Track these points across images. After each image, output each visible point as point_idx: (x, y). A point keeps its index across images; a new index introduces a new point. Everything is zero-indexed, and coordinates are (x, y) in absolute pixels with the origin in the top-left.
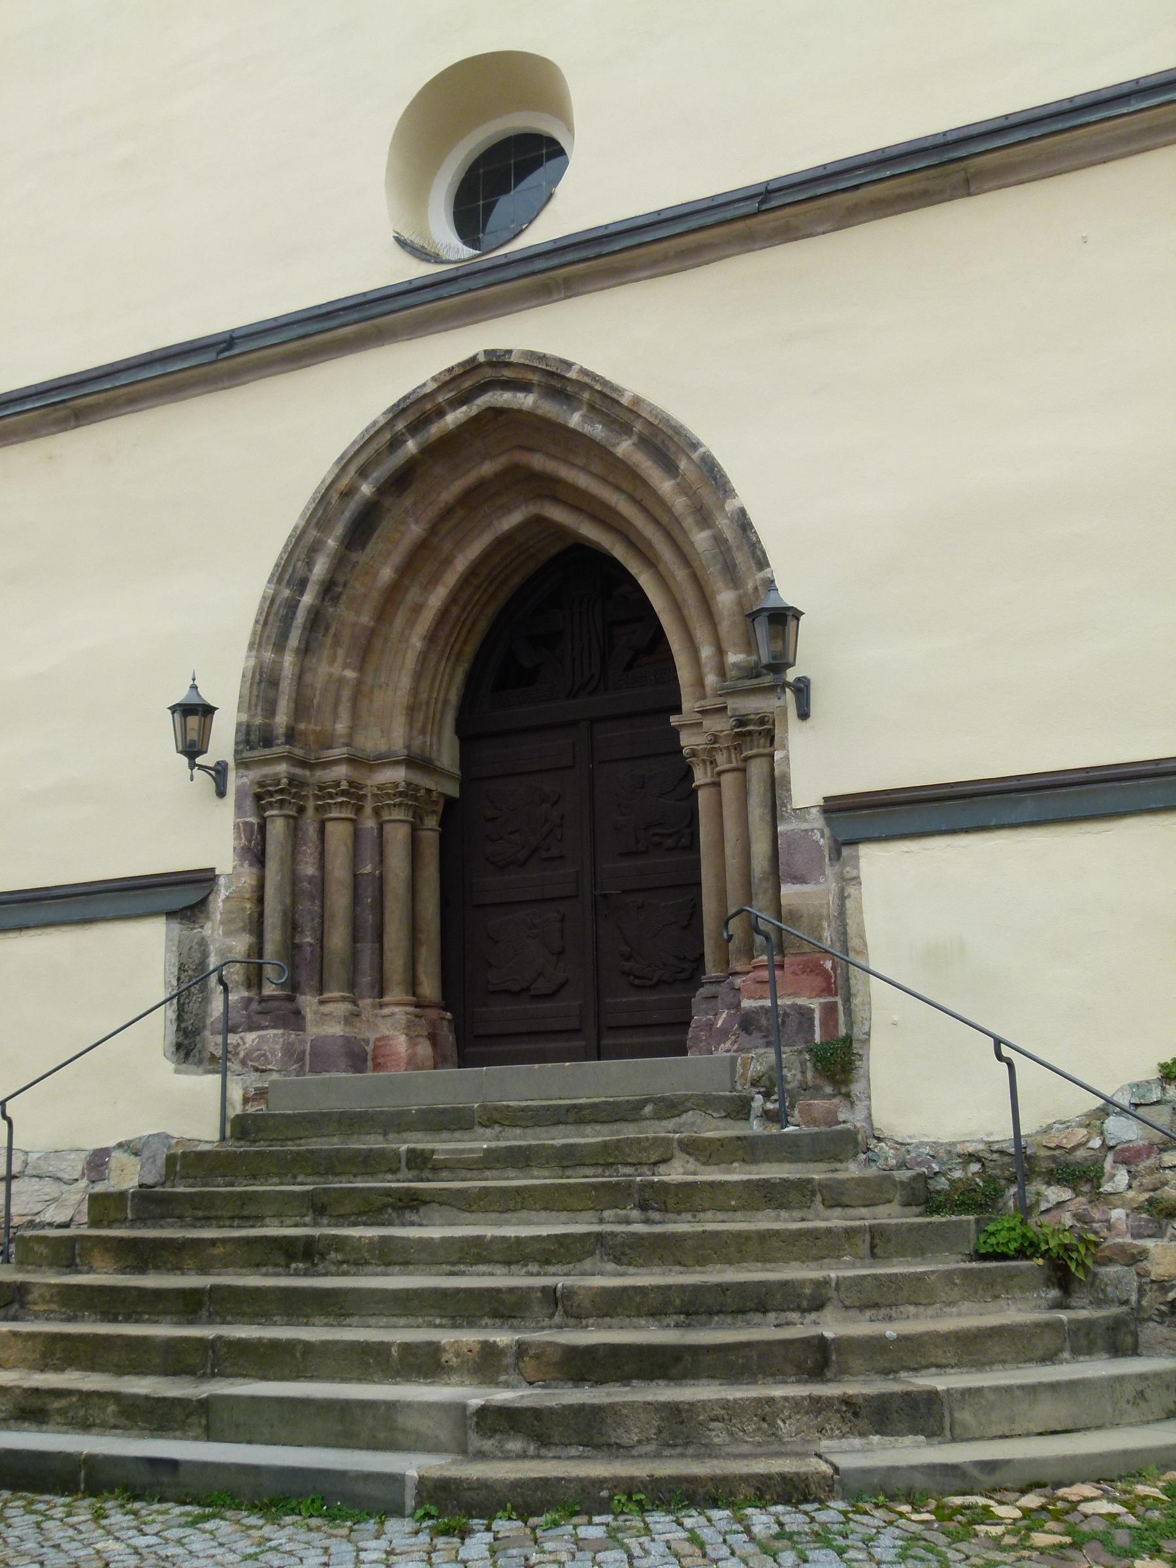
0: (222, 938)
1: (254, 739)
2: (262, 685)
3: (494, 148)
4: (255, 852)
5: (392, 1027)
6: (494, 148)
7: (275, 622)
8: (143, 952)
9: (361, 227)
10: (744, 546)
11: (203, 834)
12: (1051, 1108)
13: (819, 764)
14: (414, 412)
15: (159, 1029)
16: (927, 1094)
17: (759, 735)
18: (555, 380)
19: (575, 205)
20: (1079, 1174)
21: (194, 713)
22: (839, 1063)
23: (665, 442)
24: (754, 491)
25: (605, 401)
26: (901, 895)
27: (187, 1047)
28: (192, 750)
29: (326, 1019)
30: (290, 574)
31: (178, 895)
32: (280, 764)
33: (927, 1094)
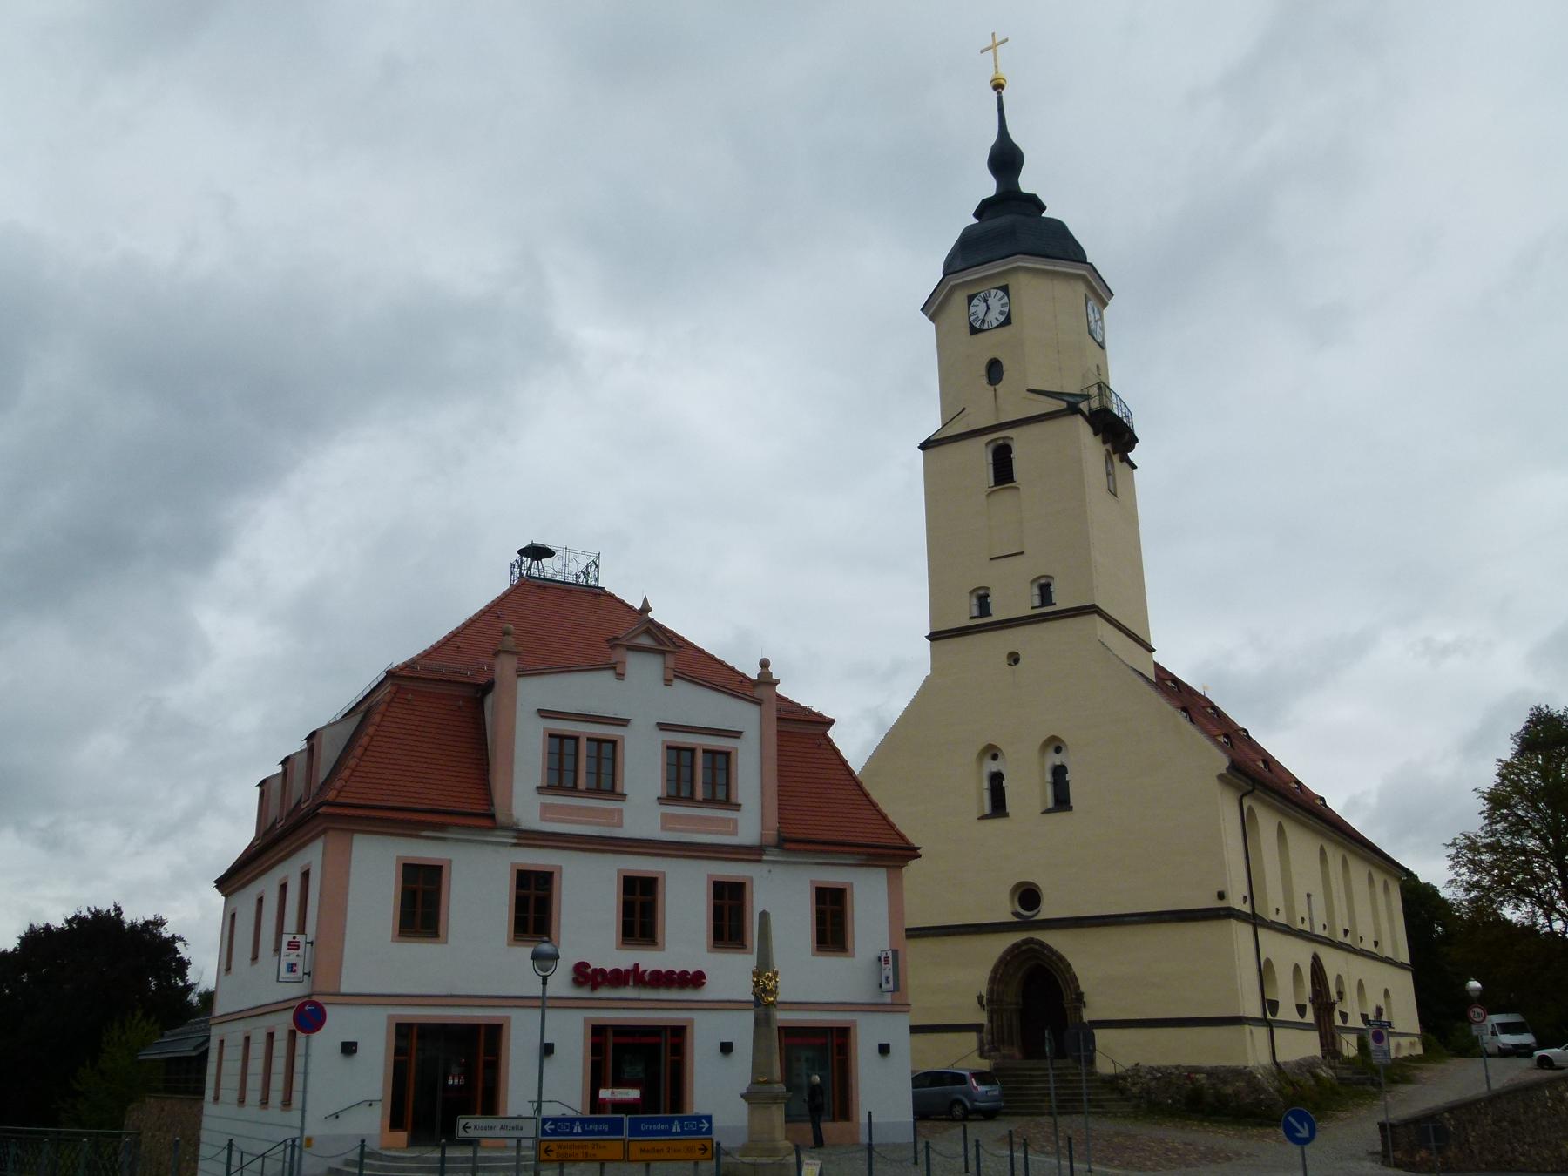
0: (987, 1037)
1: (990, 1001)
2: (991, 991)
3: (1028, 896)
4: (991, 1020)
5: (1016, 1052)
6: (1028, 896)
7: (994, 980)
8: (972, 1038)
9: (1004, 910)
10: (1074, 979)
11: (982, 1018)
12: (1119, 1070)
13: (1088, 1015)
14: (1016, 946)
15: (976, 1054)
16: (1104, 1067)
17: (1078, 1010)
18: (1042, 944)
19: (1046, 911)
20: (1124, 1079)
21: (980, 998)
22: (1091, 1061)
23: (1062, 959)
24: (1076, 969)
25: (1050, 949)
26: (1100, 1035)
27: (982, 1055)
28: (981, 1003)
29: (1005, 1051)
30: (995, 970)
31: (977, 1028)
32: (992, 1001)
33: (1104, 1067)
